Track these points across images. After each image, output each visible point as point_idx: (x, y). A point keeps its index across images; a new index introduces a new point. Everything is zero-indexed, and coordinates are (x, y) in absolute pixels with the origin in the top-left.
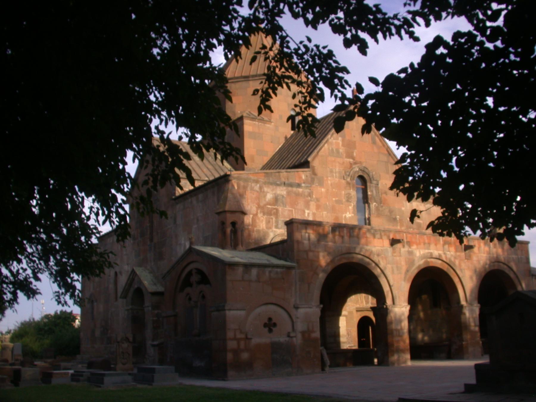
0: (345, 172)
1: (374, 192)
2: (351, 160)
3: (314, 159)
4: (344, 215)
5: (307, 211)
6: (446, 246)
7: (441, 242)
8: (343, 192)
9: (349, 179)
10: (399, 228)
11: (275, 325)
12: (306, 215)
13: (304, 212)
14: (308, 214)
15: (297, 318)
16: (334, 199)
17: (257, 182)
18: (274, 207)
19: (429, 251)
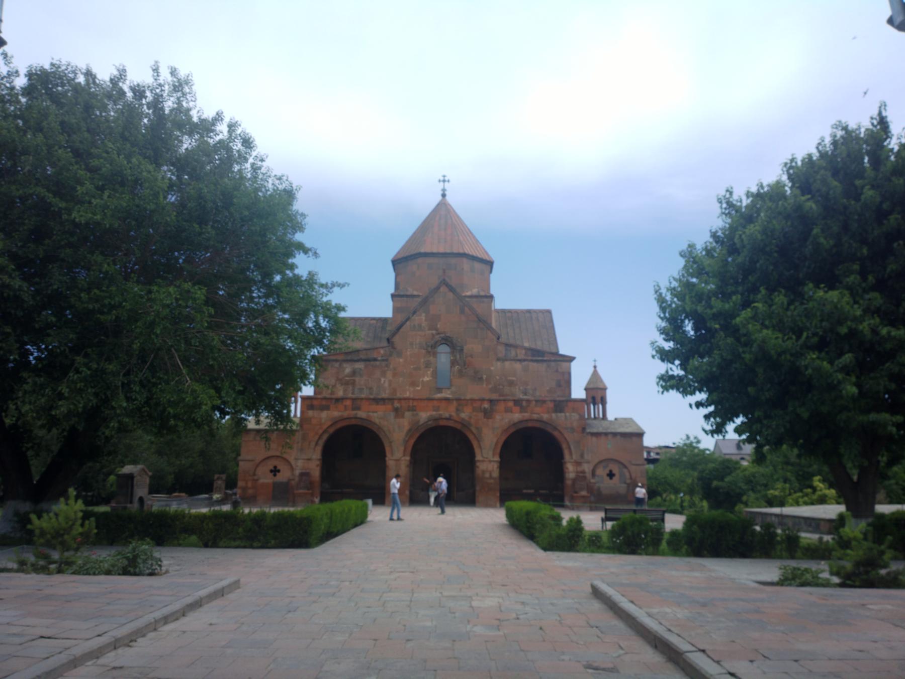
0: (426, 344)
1: (458, 356)
2: (434, 332)
3: (394, 334)
4: (421, 379)
5: (383, 380)
8: (422, 360)
9: (430, 349)
10: (484, 386)
11: (279, 471)
12: (382, 382)
13: (380, 380)
14: (384, 381)
15: (297, 466)
16: (412, 367)
17: (336, 361)
19: (438, 413)
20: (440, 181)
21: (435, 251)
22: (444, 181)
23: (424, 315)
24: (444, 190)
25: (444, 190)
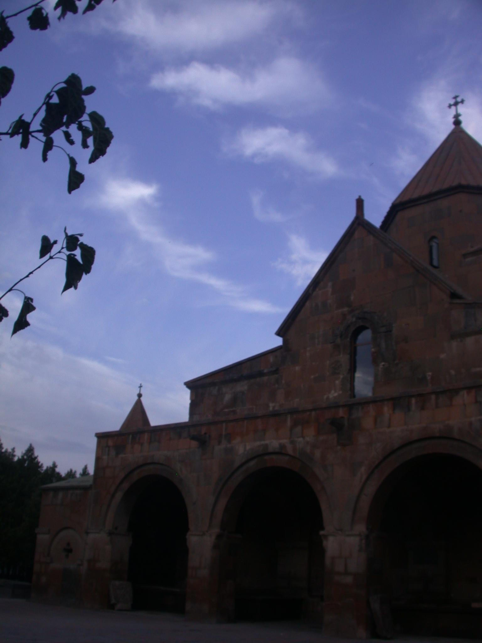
1: (383, 345)
2: (346, 309)
4: (325, 397)
5: (271, 405)
6: (298, 429)
7: (289, 423)
8: (328, 362)
9: (338, 341)
14: (274, 407)
16: (312, 377)
17: (213, 384)
18: (231, 409)
19: (263, 442)
20: (450, 106)
21: (416, 195)
22: (456, 104)
23: (330, 284)
24: (457, 116)
25: (457, 116)
